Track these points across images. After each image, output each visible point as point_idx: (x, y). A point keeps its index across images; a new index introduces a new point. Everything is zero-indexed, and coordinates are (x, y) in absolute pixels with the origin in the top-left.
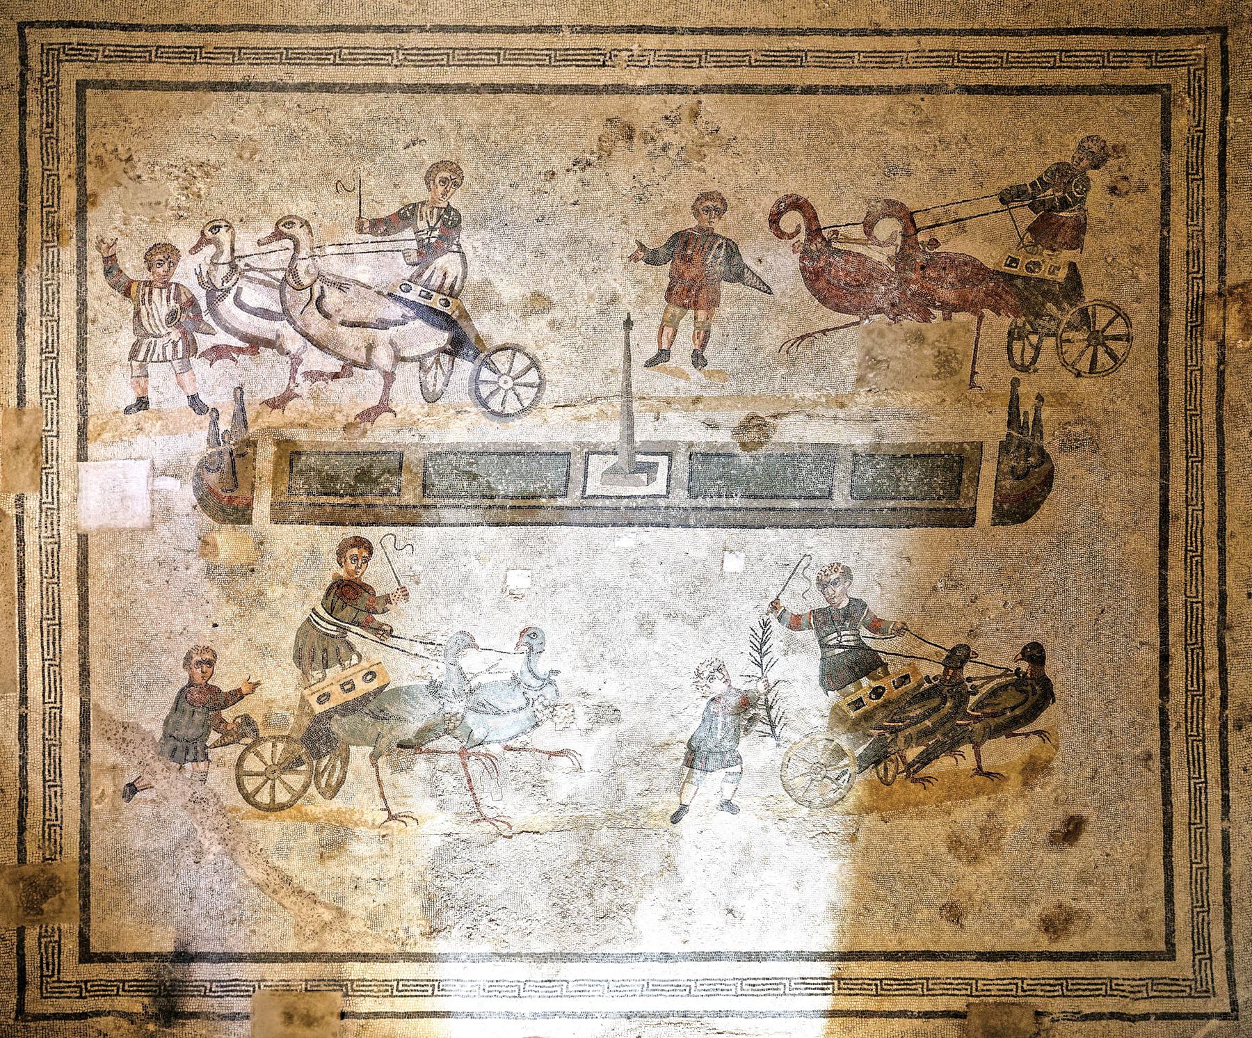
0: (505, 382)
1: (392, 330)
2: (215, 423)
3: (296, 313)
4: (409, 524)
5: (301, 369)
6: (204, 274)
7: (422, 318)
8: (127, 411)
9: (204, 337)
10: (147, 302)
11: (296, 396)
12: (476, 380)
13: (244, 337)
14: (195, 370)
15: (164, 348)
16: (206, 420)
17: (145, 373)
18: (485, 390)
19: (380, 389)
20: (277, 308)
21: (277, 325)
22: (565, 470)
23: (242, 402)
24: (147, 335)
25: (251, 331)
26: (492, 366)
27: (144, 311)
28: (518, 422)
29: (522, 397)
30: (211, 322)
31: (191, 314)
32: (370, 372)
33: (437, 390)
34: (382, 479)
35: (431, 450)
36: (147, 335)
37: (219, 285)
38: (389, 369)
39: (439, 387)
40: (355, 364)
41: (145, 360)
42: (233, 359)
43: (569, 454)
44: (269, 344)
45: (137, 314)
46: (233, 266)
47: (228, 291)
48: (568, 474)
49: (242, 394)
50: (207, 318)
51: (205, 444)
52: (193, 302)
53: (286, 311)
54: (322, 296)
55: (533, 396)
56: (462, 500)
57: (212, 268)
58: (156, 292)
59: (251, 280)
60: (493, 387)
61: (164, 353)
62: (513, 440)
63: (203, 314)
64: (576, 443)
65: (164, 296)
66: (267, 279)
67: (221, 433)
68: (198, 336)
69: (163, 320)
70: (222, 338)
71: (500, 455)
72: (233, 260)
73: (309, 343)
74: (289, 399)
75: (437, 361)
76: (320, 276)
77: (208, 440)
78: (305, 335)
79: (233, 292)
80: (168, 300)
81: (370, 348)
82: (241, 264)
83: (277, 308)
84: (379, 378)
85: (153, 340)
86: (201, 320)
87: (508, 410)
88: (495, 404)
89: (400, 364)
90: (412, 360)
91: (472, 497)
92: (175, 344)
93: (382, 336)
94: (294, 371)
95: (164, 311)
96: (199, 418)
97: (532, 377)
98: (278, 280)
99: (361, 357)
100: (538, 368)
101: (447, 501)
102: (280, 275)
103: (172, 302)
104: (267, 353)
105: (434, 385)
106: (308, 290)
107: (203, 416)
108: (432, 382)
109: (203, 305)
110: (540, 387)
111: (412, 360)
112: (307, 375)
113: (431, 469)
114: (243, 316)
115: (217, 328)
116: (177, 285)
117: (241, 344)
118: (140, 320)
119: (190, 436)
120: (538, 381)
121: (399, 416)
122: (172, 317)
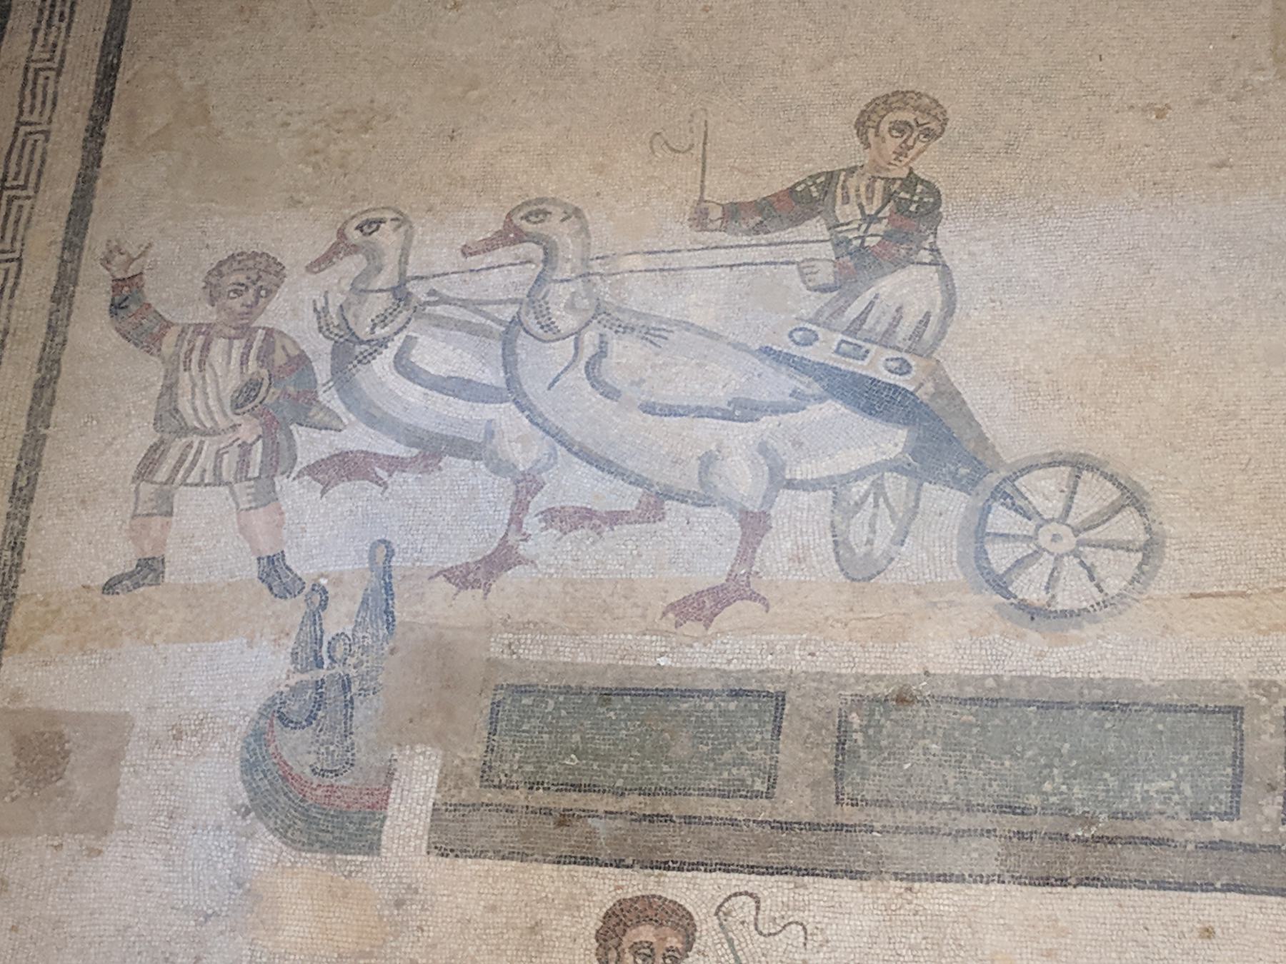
0: (1055, 538)
1: (767, 423)
2: (315, 617)
3: (534, 388)
4: (800, 872)
5: (540, 501)
6: (333, 310)
7: (841, 397)
8: (109, 587)
9: (316, 434)
10: (194, 366)
11: (520, 561)
12: (979, 534)
13: (413, 437)
14: (286, 503)
15: (219, 455)
16: (293, 611)
17: (165, 508)
18: (1000, 557)
19: (731, 549)
20: (492, 376)
21: (489, 411)
22: (1229, 750)
23: (387, 572)
24: (184, 430)
25: (425, 423)
26: (1020, 502)
27: (185, 377)
28: (1090, 630)
29: (1100, 572)
30: (337, 405)
31: (291, 389)
32: (706, 512)
33: (878, 554)
34: (727, 756)
35: (860, 689)
36: (184, 430)
37: (364, 332)
38: (754, 506)
39: (881, 544)
40: (668, 494)
41: (170, 480)
42: (378, 481)
43: (1236, 712)
44: (464, 448)
45: (170, 388)
46: (400, 294)
47: (383, 343)
48: (1237, 760)
49: (390, 554)
50: (329, 398)
51: (282, 663)
52: (301, 362)
53: (512, 382)
54: (602, 352)
55: (1131, 571)
56: (942, 816)
57: (354, 299)
58: (219, 345)
59: (439, 322)
60: (1022, 550)
61: (217, 468)
62: (1078, 671)
63: (321, 390)
64: (1256, 685)
65: (236, 354)
66: (477, 319)
67: (326, 639)
68: (301, 434)
69: (227, 402)
70: (357, 438)
71: (1045, 706)
72: (403, 280)
73: (561, 450)
74: (506, 566)
75: (878, 488)
76: (599, 310)
77: (294, 654)
78: (557, 435)
79: (398, 341)
80: (244, 362)
81: (707, 462)
82: (419, 291)
83: (492, 376)
84: (730, 525)
85: (196, 440)
86: (313, 400)
87: (1064, 601)
88: (1030, 588)
89: (785, 497)
90: (815, 485)
91: (969, 808)
92: (245, 449)
93: (739, 436)
94: (520, 507)
95: (232, 383)
96: (281, 605)
97: (1127, 526)
98: (501, 323)
99: (686, 479)
100: (1141, 510)
101: (900, 816)
102: (508, 313)
103: (252, 365)
104: (455, 466)
105: (870, 542)
106: (570, 341)
107: (288, 603)
108: (865, 534)
109: (322, 370)
110: (1151, 549)
111: (815, 485)
112: (550, 516)
113: (859, 737)
114: (413, 393)
115: (348, 417)
116: (269, 332)
117: (400, 450)
118: (174, 399)
119: (250, 645)
120: (1143, 537)
121: (774, 609)
122: (247, 395)
